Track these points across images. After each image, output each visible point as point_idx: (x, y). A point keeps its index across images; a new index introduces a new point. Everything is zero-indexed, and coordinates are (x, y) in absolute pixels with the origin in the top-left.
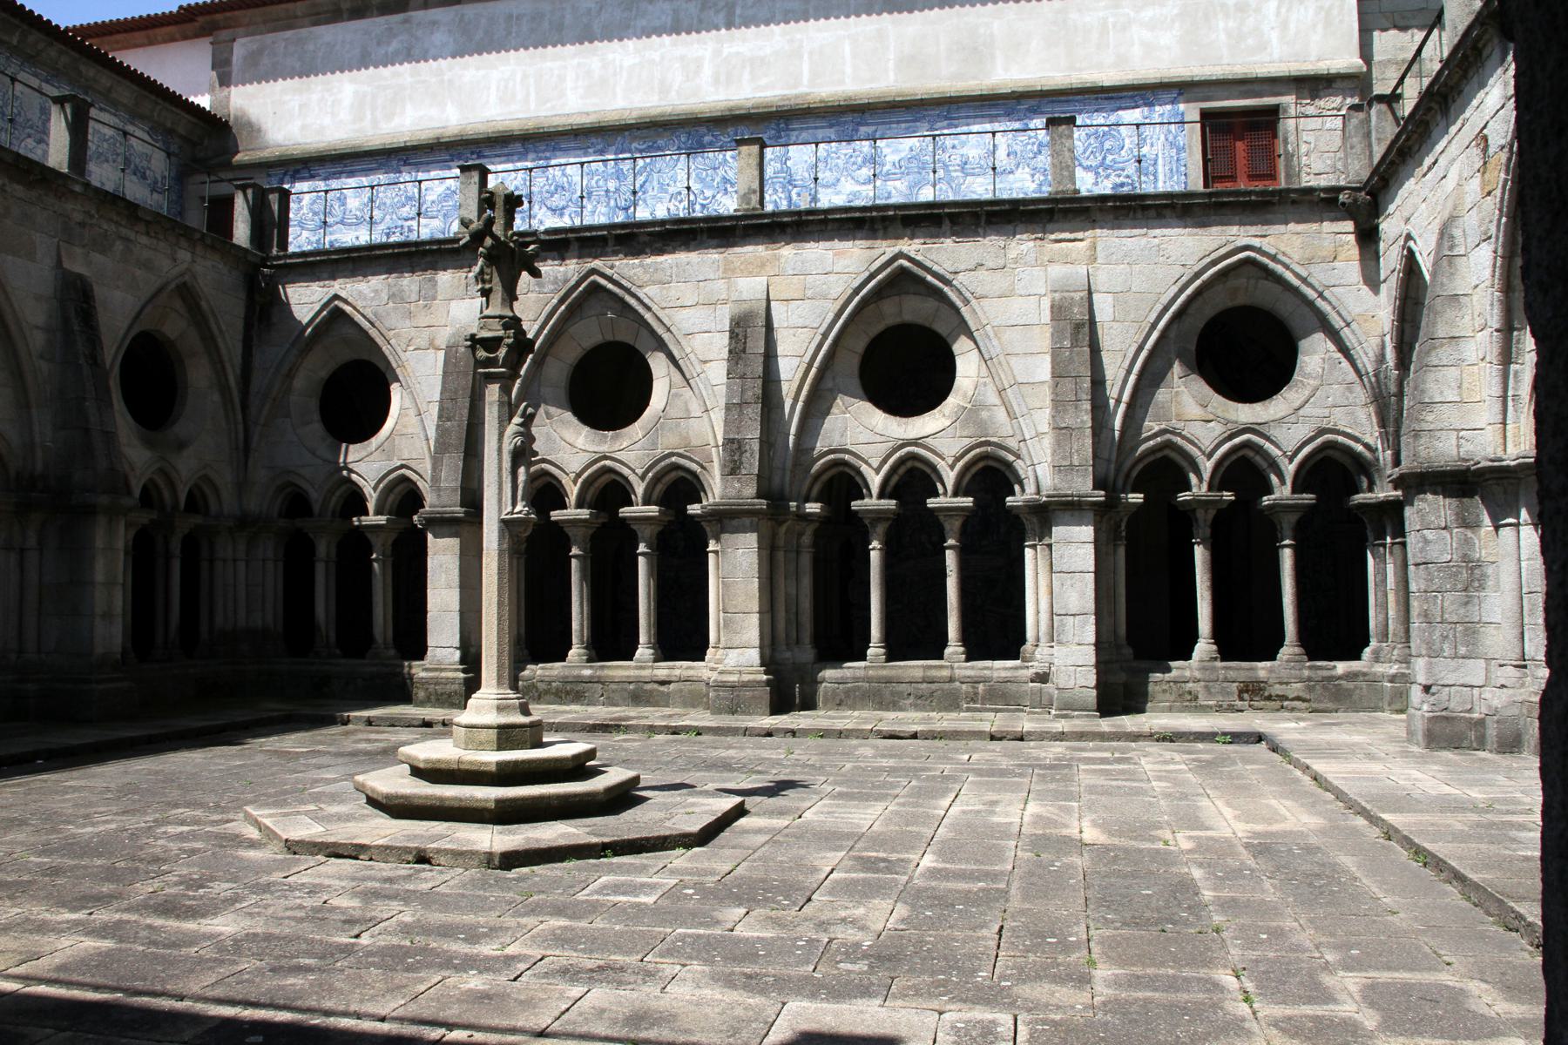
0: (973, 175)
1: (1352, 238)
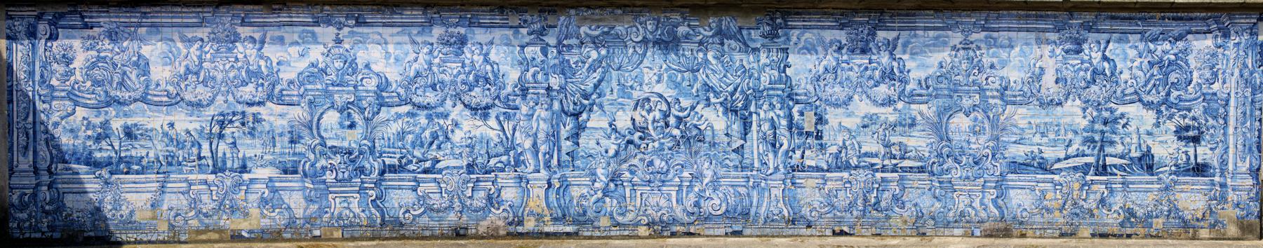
0: (1014, 103)
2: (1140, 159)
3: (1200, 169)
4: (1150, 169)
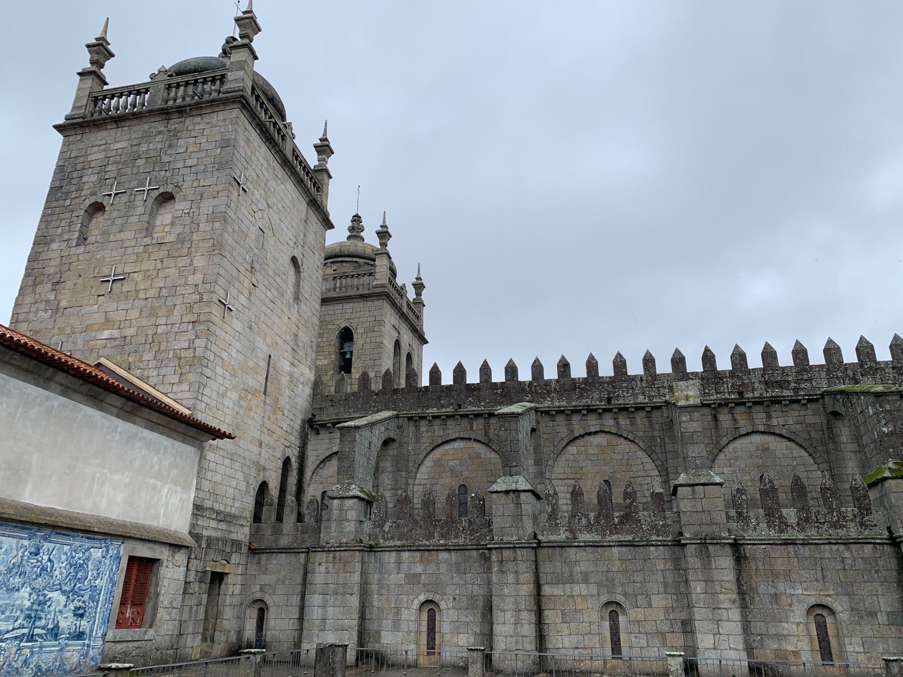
2: (52, 629)
3: (80, 636)
4: (56, 637)
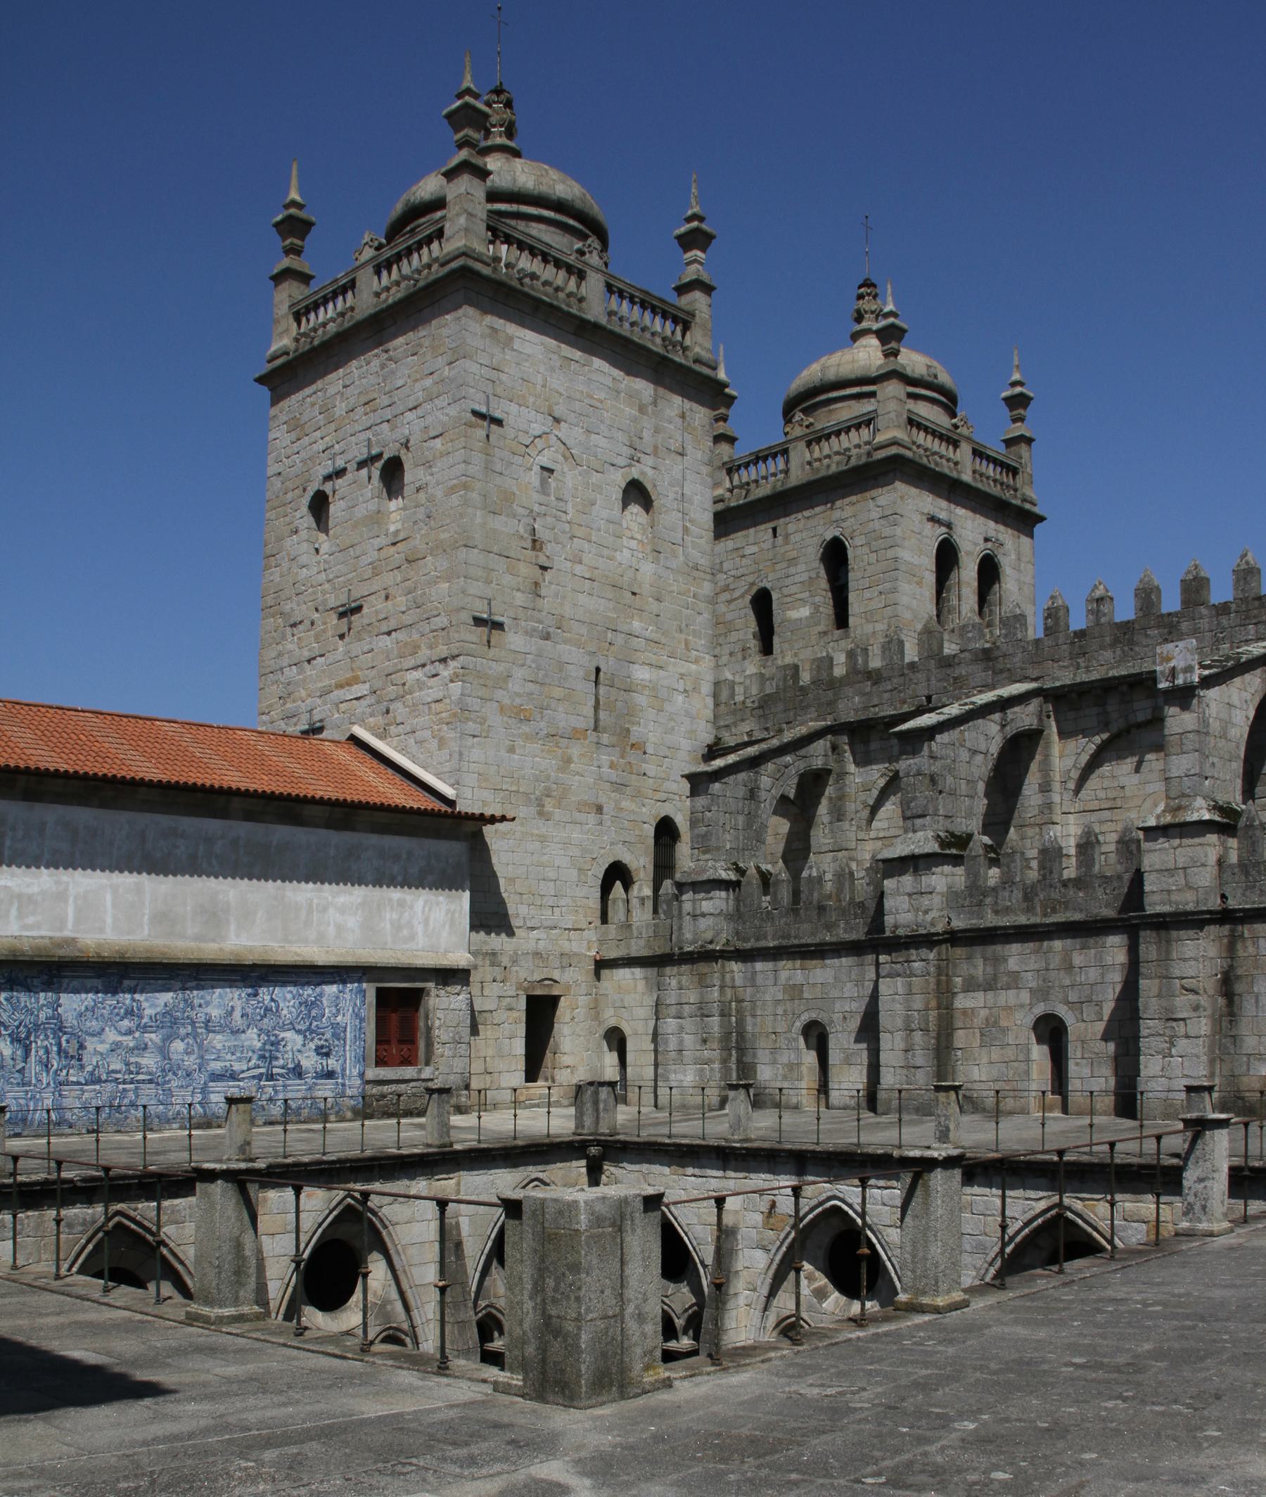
0: (214, 1032)
1: (584, 1170)
3: (330, 1075)
